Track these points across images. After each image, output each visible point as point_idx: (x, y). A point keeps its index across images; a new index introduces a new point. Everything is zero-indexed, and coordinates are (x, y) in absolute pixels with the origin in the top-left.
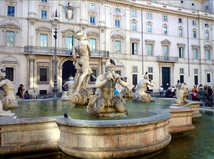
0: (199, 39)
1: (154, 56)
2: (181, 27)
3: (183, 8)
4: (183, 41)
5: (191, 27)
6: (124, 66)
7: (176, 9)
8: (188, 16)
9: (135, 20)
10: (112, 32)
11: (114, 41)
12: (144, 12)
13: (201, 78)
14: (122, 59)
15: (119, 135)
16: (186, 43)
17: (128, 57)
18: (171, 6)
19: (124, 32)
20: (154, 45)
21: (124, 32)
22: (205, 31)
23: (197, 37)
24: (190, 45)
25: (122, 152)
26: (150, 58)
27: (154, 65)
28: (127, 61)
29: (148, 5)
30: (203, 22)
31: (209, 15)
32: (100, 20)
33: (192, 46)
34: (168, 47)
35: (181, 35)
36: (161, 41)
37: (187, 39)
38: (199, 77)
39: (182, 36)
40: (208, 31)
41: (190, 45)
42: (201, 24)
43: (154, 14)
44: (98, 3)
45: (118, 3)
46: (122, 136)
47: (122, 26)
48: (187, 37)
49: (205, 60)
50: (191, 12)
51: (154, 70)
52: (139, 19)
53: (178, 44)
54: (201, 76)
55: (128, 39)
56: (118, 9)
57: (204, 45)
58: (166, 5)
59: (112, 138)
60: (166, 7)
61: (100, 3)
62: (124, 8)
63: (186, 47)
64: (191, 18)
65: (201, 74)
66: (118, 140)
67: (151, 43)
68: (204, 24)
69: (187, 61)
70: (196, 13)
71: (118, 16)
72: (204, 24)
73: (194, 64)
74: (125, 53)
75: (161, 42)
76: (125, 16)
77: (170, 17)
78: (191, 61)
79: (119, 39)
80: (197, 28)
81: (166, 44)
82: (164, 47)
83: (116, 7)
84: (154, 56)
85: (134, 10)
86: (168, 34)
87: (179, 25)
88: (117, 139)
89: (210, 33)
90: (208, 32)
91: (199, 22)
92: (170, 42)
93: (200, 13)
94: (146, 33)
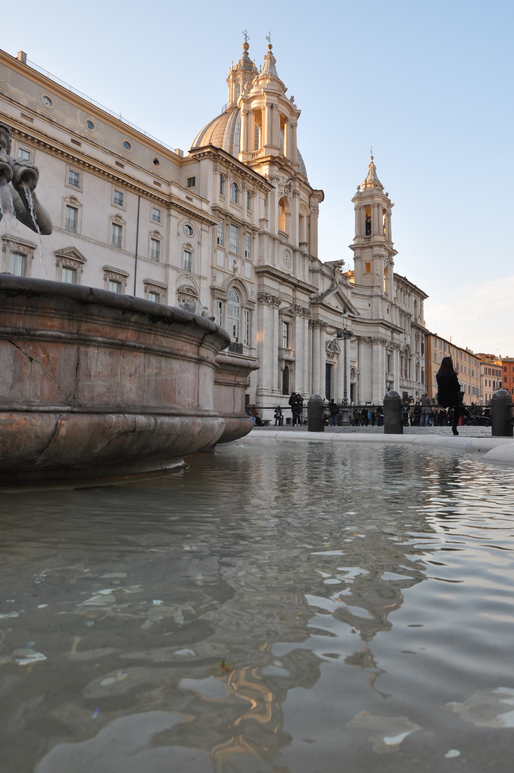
0: (167, 266)
2: (120, 217)
7: (111, 161)
8: (141, 192)
15: (82, 349)
16: (132, 273)
18: (96, 145)
20: (33, 258)
22: (184, 245)
23: (162, 259)
24: (141, 278)
25: (96, 419)
30: (181, 217)
31: (196, 203)
33: (147, 283)
34: (76, 274)
36: (57, 248)
37: (134, 259)
39: (120, 247)
40: (190, 245)
41: (141, 278)
42: (174, 221)
46: (92, 351)
48: (134, 252)
50: (149, 180)
57: (179, 285)
58: (81, 137)
59: (51, 355)
60: (79, 144)
64: (148, 198)
66: (77, 368)
67: (21, 249)
68: (181, 224)
70: (164, 188)
72: (181, 224)
75: (55, 252)
77: (88, 179)
80: (162, 231)
82: (64, 271)
86: (78, 231)
87: (115, 211)
88: (73, 362)
89: (195, 255)
90: (191, 249)
91: (169, 215)
92: (84, 259)
93: (175, 191)
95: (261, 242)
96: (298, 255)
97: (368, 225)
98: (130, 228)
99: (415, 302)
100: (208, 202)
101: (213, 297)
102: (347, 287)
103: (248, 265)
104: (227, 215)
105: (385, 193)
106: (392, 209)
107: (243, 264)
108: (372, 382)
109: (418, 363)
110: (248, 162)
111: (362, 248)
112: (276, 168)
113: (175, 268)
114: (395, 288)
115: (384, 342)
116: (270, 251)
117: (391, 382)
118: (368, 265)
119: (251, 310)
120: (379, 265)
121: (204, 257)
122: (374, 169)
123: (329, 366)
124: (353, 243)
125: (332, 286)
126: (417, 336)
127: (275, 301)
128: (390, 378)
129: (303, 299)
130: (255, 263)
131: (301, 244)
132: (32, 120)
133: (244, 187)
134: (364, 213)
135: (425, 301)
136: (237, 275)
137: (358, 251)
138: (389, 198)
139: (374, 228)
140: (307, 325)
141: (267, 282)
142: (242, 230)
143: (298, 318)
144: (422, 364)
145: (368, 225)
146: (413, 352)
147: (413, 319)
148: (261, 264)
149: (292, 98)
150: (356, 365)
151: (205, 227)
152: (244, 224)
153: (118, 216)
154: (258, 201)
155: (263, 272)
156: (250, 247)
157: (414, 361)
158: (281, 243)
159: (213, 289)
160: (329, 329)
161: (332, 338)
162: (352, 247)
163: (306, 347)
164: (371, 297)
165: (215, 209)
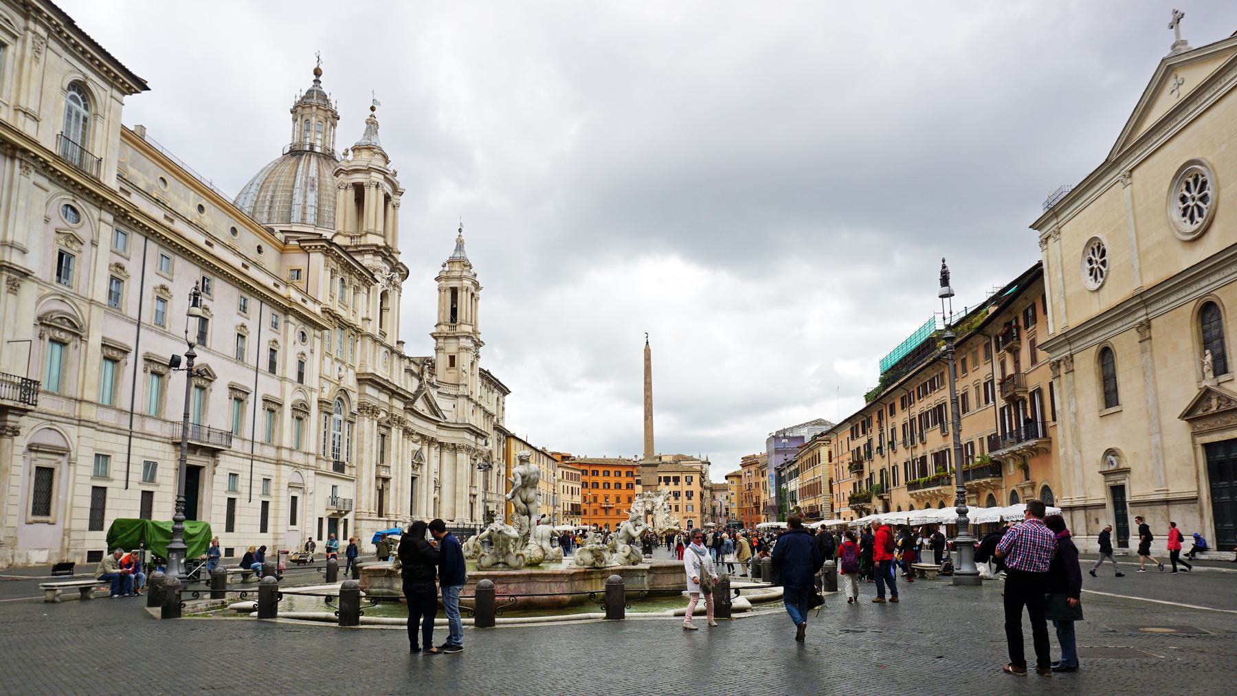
0: (283, 379)
1: (165, 421)
3: (255, 264)
4: (244, 378)
5: (268, 335)
6: (69, 451)
9: (122, 268)
10: (41, 298)
11: (47, 338)
12: (153, 247)
13: (277, 510)
14: (68, 419)
17: (89, 413)
19: (83, 308)
26: (152, 427)
27: (161, 455)
28: (82, 428)
29: (167, 223)
30: (297, 323)
31: (310, 305)
32: (9, 239)
35: (240, 357)
38: (271, 506)
43: (180, 263)
44: (8, 161)
45: (84, 188)
47: (82, 280)
49: (291, 450)
51: (159, 471)
52: (133, 268)
53: (233, 388)
54: (277, 502)
55: (95, 341)
56: (73, 209)
58: (215, 239)
61: (17, 163)
62: (95, 213)
63: (251, 398)
65: (278, 497)
69: (247, 449)
70: (282, 290)
71: (73, 238)
73: (264, 460)
74: (79, 397)
76: (94, 244)
78: (257, 451)
79: (63, 336)
83: (68, 198)
84: (165, 421)
85: (122, 229)
87: (240, 320)
91: (287, 321)
92: (215, 377)
94: (149, 328)
95: (363, 345)
96: (395, 357)
97: (454, 312)
98: (251, 338)
100: (320, 303)
101: (321, 411)
102: (432, 385)
103: (351, 371)
104: (336, 317)
106: (480, 293)
108: (455, 497)
110: (347, 247)
111: (446, 338)
112: (380, 258)
113: (291, 381)
114: (479, 384)
115: (468, 449)
117: (475, 496)
118: (452, 359)
119: (352, 422)
120: (464, 360)
122: (460, 246)
123: (413, 479)
124: (434, 330)
125: (420, 387)
126: (499, 440)
127: (374, 411)
128: (474, 492)
129: (398, 404)
130: (357, 370)
131: (398, 342)
132: (172, 221)
133: (350, 283)
134: (449, 294)
136: (343, 385)
137: (441, 340)
139: (461, 315)
141: (369, 390)
142: (347, 331)
143: (393, 429)
144: (503, 472)
145: (454, 312)
146: (495, 459)
148: (363, 371)
151: (318, 333)
152: (350, 326)
153: (243, 326)
154: (362, 297)
155: (366, 380)
156: (353, 351)
157: (495, 469)
158: (382, 344)
159: (320, 402)
160: (416, 437)
161: (417, 447)
162: (432, 335)
164: (456, 396)
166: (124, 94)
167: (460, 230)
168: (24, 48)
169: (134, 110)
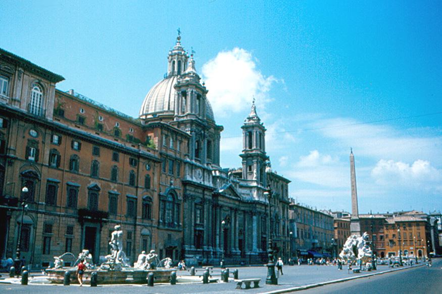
5: (128, 168)
21: (39, 168)
51: (75, 230)
77: (103, 151)
81: (94, 192)
99: (282, 186)
105: (261, 123)
107: (175, 180)
109: (285, 224)
116: (190, 171)
117: (265, 238)
121: (155, 180)
135: (289, 184)
138: (264, 125)
140: (211, 207)
147: (281, 196)
149: (204, 84)
150: (243, 229)
151: (156, 165)
155: (185, 184)
159: (159, 195)
162: (241, 156)
163: (210, 221)
165: (161, 154)
166: (55, 83)
167: (253, 102)
168: (15, 77)
169: (59, 86)
